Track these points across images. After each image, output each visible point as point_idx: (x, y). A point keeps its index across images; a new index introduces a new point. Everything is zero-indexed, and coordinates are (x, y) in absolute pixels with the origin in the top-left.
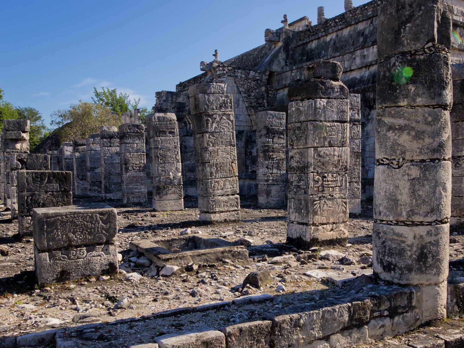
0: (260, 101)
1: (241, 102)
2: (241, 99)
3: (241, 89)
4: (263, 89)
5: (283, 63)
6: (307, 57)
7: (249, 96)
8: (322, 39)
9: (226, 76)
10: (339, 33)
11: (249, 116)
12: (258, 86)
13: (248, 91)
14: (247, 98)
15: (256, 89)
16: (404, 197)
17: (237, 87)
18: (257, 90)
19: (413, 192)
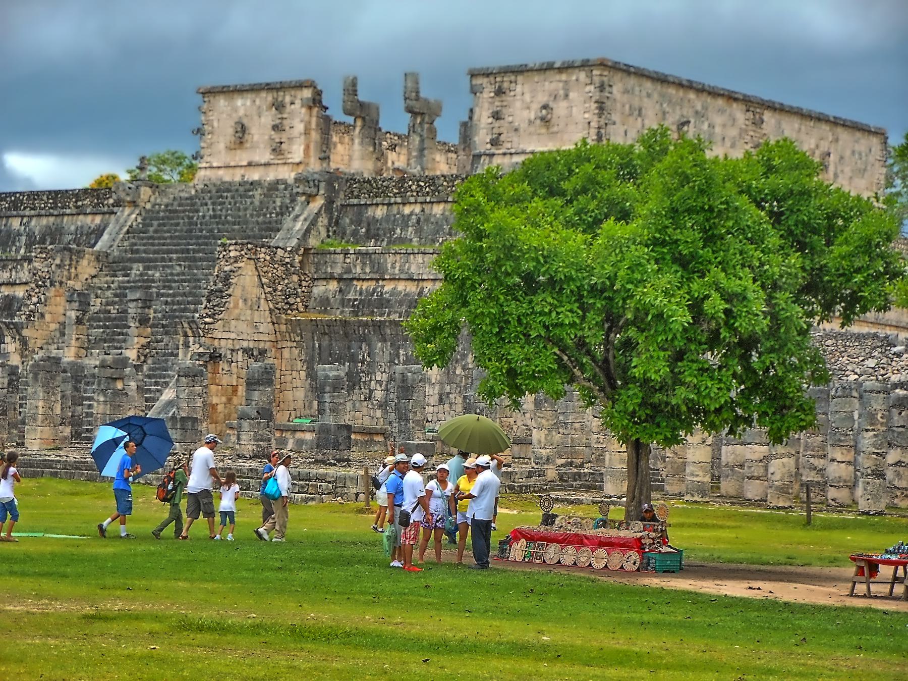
0: (291, 300)
1: (262, 301)
2: (263, 296)
3: (264, 280)
4: (295, 278)
5: (324, 234)
6: (368, 231)
7: (275, 290)
8: (395, 209)
9: (245, 259)
10: (427, 207)
11: (274, 323)
12: (288, 274)
13: (273, 283)
14: (271, 294)
15: (284, 279)
16: (543, 440)
17: (259, 275)
18: (286, 281)
19: (546, 439)
